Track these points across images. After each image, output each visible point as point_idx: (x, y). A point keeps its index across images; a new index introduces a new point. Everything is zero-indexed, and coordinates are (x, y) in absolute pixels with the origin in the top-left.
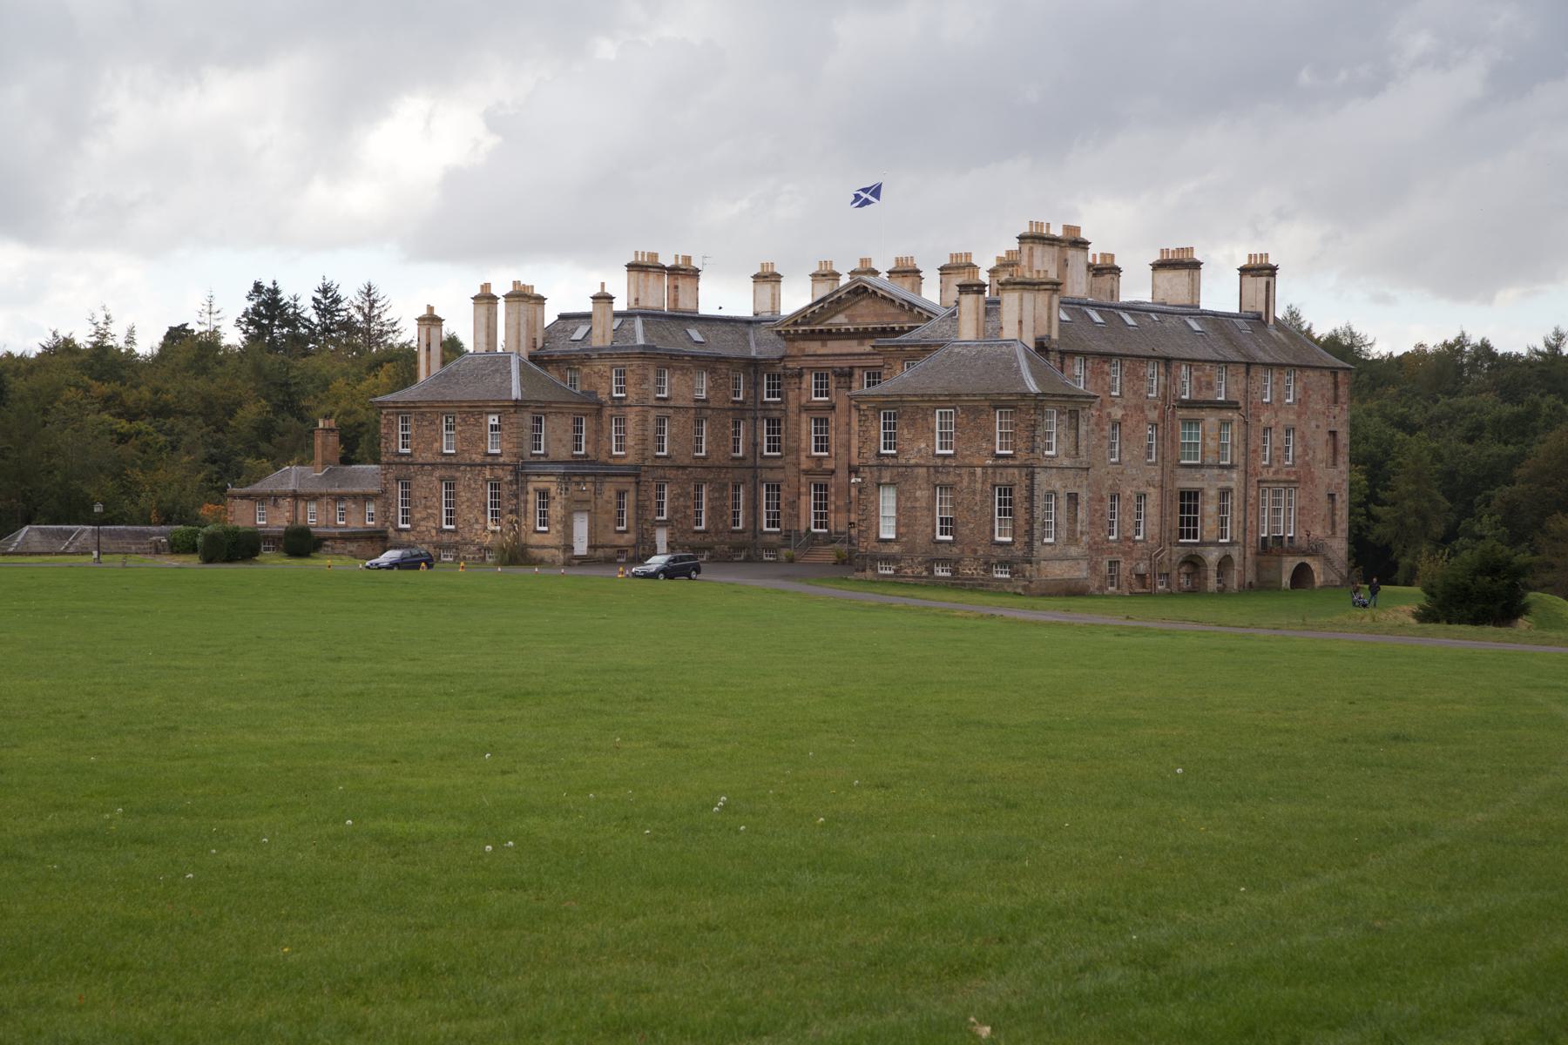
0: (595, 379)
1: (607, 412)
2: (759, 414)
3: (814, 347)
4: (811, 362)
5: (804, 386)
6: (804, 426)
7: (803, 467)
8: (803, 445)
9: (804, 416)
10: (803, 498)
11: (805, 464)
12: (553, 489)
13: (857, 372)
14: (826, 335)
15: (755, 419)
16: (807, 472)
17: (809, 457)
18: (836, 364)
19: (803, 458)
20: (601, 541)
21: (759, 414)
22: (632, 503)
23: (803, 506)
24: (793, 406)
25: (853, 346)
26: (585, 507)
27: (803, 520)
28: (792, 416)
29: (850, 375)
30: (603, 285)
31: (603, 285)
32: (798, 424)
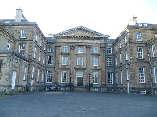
0: (14, 33)
1: (17, 42)
2: (47, 55)
3: (65, 40)
4: (64, 44)
5: (61, 49)
6: (60, 58)
7: (59, 67)
8: (60, 62)
9: (60, 56)
10: (59, 75)
11: (60, 67)
12: (5, 60)
13: (76, 46)
14: (71, 37)
15: (46, 56)
16: (61, 69)
17: (61, 65)
18: (71, 44)
19: (60, 65)
20: (20, 84)
21: (47, 55)
22: (75, 64)
23: (59, 77)
24: (57, 53)
25: (76, 41)
26: (17, 70)
27: (59, 80)
28: (57, 56)
29: (75, 47)
30: (20, 7)
31: (20, 7)
32: (59, 57)
